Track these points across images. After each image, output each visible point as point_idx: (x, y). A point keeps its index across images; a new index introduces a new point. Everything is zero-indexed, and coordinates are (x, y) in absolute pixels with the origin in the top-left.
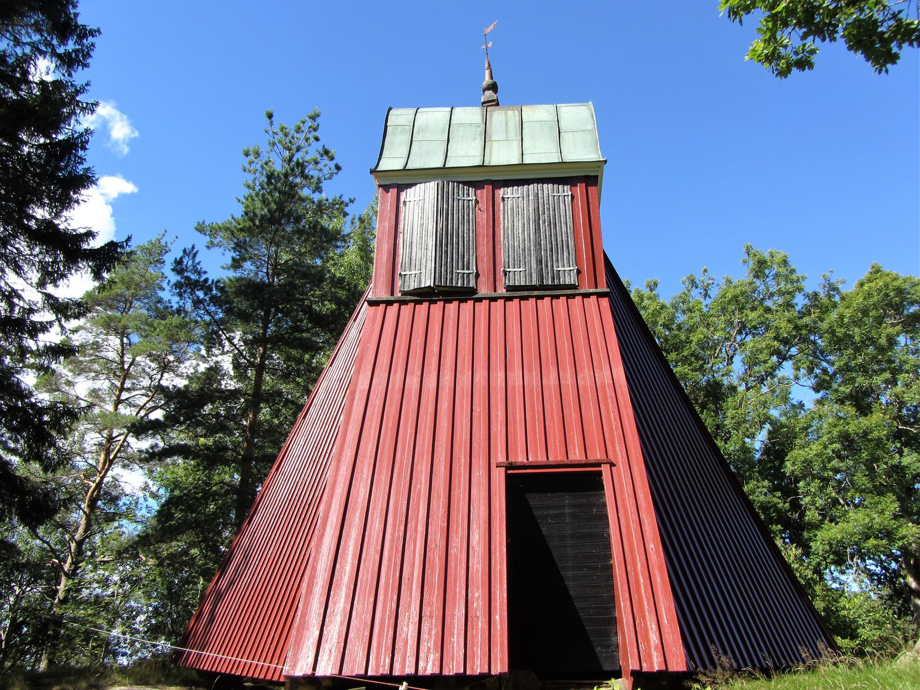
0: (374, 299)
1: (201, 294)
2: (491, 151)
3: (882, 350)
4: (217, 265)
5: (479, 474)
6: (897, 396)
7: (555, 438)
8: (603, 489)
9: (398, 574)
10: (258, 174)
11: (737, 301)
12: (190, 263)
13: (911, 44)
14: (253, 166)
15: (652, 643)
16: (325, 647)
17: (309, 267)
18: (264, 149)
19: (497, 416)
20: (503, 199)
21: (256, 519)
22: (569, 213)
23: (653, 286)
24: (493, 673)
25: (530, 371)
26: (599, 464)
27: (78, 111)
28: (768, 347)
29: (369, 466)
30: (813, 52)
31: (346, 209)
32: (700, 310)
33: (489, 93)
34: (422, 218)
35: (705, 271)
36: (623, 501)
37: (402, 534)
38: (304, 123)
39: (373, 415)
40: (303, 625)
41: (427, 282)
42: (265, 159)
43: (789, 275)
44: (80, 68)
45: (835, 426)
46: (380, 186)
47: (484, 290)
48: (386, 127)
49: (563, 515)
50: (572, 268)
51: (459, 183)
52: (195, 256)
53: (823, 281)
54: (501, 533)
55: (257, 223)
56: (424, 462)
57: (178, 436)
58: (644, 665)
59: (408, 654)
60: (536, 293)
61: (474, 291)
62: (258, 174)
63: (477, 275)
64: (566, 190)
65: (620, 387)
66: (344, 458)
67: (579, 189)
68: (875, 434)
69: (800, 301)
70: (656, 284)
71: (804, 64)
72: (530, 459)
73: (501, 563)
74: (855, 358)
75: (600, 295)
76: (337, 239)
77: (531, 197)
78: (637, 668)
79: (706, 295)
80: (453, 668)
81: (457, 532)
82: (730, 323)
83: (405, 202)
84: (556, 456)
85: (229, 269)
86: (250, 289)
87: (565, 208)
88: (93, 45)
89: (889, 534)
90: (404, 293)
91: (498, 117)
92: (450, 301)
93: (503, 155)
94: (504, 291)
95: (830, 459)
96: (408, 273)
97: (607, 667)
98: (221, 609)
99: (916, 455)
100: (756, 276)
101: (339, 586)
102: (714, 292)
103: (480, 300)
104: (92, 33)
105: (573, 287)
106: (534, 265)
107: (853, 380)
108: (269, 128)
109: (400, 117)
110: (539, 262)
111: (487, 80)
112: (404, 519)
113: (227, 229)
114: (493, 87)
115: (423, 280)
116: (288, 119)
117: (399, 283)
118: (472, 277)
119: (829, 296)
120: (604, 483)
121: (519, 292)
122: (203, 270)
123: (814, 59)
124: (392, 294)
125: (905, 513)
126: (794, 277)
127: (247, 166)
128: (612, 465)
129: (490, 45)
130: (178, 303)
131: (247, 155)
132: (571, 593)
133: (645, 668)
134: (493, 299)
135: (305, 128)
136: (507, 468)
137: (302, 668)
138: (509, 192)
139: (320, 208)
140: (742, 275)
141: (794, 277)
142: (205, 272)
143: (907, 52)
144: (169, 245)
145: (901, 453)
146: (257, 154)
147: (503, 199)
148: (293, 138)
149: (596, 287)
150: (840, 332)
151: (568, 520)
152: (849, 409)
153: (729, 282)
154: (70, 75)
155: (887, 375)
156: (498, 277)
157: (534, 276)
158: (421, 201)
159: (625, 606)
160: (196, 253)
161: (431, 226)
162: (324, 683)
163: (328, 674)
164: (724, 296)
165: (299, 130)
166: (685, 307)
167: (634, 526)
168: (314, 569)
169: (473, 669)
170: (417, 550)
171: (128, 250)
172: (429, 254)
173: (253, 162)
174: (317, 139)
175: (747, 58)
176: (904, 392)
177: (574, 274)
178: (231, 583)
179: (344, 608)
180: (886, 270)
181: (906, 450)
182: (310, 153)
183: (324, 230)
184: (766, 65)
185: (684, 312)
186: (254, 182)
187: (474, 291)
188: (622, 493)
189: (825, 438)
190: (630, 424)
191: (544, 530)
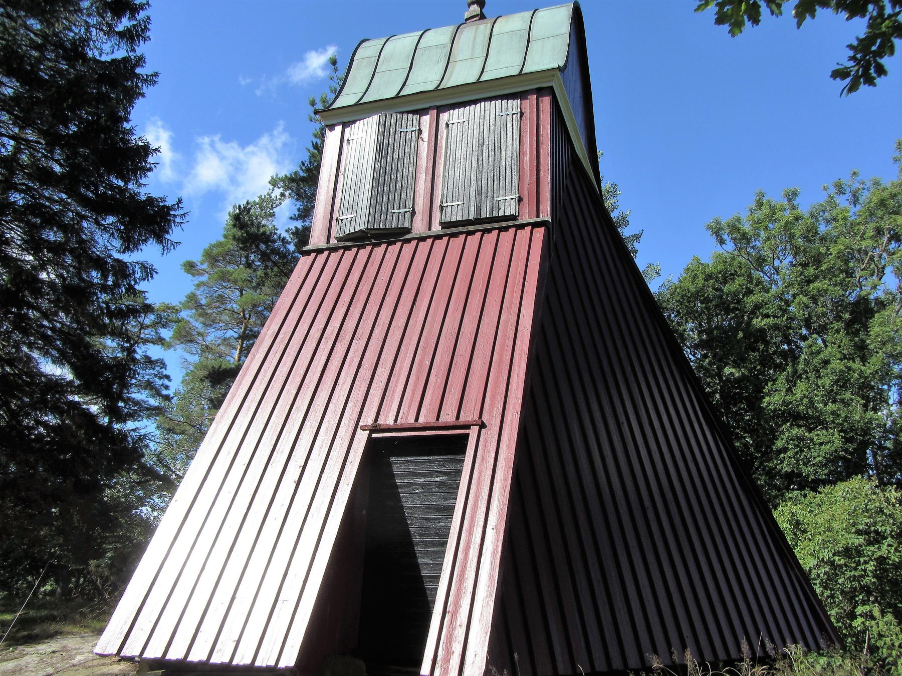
11: (885, 206)
23: (792, 196)
26: (467, 427)
27: (140, 85)
32: (845, 218)
41: (361, 226)
47: (419, 227)
61: (408, 231)
63: (413, 213)
64: (513, 105)
70: (795, 194)
79: (855, 201)
82: (879, 232)
88: (149, 18)
96: (345, 217)
102: (864, 197)
104: (142, 7)
105: (513, 218)
108: (334, 75)
110: (479, 193)
118: (408, 216)
128: (483, 426)
147: (447, 125)
149: (538, 216)
153: (877, 183)
154: (134, 50)
157: (472, 208)
166: (827, 215)
177: (514, 203)
185: (828, 222)
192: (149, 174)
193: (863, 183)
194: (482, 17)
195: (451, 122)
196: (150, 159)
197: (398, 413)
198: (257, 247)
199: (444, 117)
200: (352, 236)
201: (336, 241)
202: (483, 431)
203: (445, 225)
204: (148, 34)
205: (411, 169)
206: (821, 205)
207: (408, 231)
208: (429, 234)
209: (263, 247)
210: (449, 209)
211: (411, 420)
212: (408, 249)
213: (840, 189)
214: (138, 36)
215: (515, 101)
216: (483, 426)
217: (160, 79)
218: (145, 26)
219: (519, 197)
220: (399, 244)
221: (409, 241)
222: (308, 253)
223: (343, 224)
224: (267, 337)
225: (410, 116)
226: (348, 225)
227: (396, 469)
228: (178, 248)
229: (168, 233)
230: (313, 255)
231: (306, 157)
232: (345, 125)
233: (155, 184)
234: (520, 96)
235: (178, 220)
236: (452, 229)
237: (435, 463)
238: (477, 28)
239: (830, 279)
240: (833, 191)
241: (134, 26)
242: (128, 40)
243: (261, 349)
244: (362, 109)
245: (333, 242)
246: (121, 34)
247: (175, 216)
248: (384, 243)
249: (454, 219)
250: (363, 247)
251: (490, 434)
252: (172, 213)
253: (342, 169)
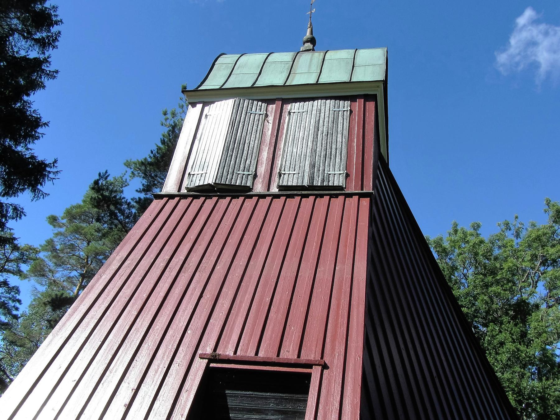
11: (540, 240)
23: (476, 227)
26: (310, 366)
32: (512, 246)
35: (517, 217)
41: (210, 180)
44: (51, 49)
47: (259, 188)
48: (214, 64)
50: (342, 172)
61: (250, 189)
63: (255, 176)
64: (345, 105)
67: (358, 104)
70: (479, 226)
75: (362, 195)
79: (518, 236)
82: (534, 257)
88: (59, 33)
102: (523, 234)
104: (56, 23)
105: (340, 188)
110: (313, 166)
114: (312, 41)
127: (164, 122)
128: (325, 367)
136: (210, 361)
138: (295, 107)
140: (544, 221)
144: (128, 181)
149: (362, 189)
153: (533, 225)
154: (44, 53)
160: (108, 176)
164: (529, 237)
166: (500, 243)
171: (54, 170)
185: (500, 247)
188: (327, 403)
190: (358, 322)
192: (36, 141)
193: (522, 224)
194: (313, 50)
195: (293, 111)
196: (40, 130)
197: (238, 346)
198: (108, 207)
199: (288, 107)
200: (200, 188)
201: (186, 191)
202: (325, 371)
203: (281, 188)
204: (57, 43)
205: (256, 142)
206: (497, 235)
207: (250, 189)
208: (268, 193)
209: (112, 207)
210: (286, 176)
211: (253, 354)
212: (250, 203)
213: (508, 227)
214: (50, 44)
215: (346, 102)
216: (325, 367)
217: (59, 75)
218: (56, 38)
219: (347, 173)
220: (241, 199)
221: (251, 197)
222: (160, 197)
223: (194, 179)
224: (115, 262)
225: (260, 103)
226: (198, 179)
227: (231, 402)
228: (46, 198)
229: (41, 184)
230: (165, 199)
231: (165, 130)
232: (205, 104)
233: (39, 149)
234: (352, 98)
235: (51, 175)
236: (288, 191)
237: (271, 400)
238: (313, 55)
239: (502, 286)
240: (504, 228)
241: (48, 37)
242: (41, 45)
243: (108, 272)
244: (222, 93)
245: (184, 191)
246: (37, 41)
247: (49, 172)
249: (290, 184)
250: (210, 197)
251: (333, 375)
252: (48, 169)
253: (198, 136)
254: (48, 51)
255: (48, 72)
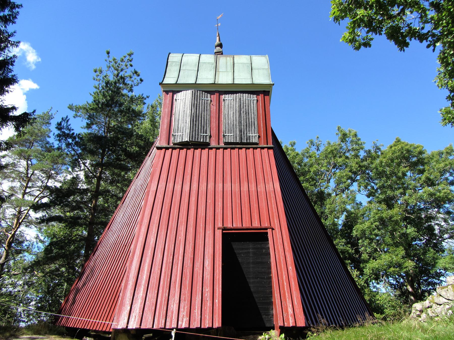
0: (160, 146)
1: (70, 141)
2: (218, 76)
3: (399, 178)
4: (79, 126)
5: (209, 232)
6: (405, 200)
7: (246, 216)
8: (268, 241)
9: (169, 280)
10: (101, 82)
11: (333, 153)
12: (65, 125)
13: (415, 39)
14: (99, 77)
15: (289, 313)
16: (133, 315)
17: (126, 129)
18: (105, 69)
19: (218, 205)
20: (224, 100)
21: (97, 253)
22: (255, 108)
23: (293, 144)
24: (214, 327)
25: (235, 183)
26: (266, 229)
27: (9, 46)
28: (346, 175)
29: (156, 228)
30: (371, 39)
31: (145, 101)
32: (315, 157)
33: (218, 48)
34: (184, 108)
36: (278, 246)
37: (171, 261)
38: (125, 57)
39: (158, 203)
40: (122, 304)
41: (186, 139)
42: (105, 74)
43: (357, 142)
45: (377, 214)
46: (164, 91)
49: (249, 252)
51: (203, 91)
52: (68, 121)
53: (373, 145)
54: (219, 261)
55: (100, 106)
56: (183, 226)
57: (56, 212)
58: (286, 323)
59: (173, 318)
60: (239, 146)
61: (208, 144)
62: (101, 82)
63: (210, 137)
64: (254, 97)
65: (278, 193)
66: (143, 223)
67: (261, 97)
68: (395, 218)
69: (362, 154)
70: (294, 143)
71: (367, 44)
72: (234, 226)
73: (219, 275)
74: (387, 182)
75: (269, 148)
76: (140, 116)
77: (237, 100)
78: (282, 325)
79: (318, 150)
80: (195, 325)
81: (198, 260)
82: (329, 163)
83: (176, 99)
84: (246, 224)
85: (85, 128)
86: (95, 139)
87: (254, 106)
88: (18, 12)
89: (399, 266)
90: (175, 144)
91: (222, 60)
92: (197, 149)
93: (225, 79)
94: (223, 144)
95: (374, 230)
96: (177, 134)
97: (268, 325)
98: (79, 297)
99: (413, 228)
100: (343, 142)
101: (140, 285)
102: (322, 148)
103: (211, 148)
104: (18, 6)
105: (256, 144)
106: (238, 133)
107: (386, 192)
108: (107, 59)
109: (175, 58)
110: (241, 131)
111: (217, 42)
112: (172, 253)
113: (85, 108)
114: (220, 45)
115: (184, 138)
116: (117, 55)
117: (172, 139)
119: (376, 152)
120: (269, 238)
121: (230, 146)
122: (72, 128)
123: (371, 43)
124: (169, 144)
125: (408, 256)
126: (360, 142)
127: (96, 77)
128: (273, 229)
129: (219, 25)
130: (58, 144)
131: (96, 72)
132: (252, 290)
133: (286, 325)
134: (218, 148)
135: (126, 60)
136: (223, 230)
137: (121, 325)
139: (132, 100)
140: (335, 140)
141: (360, 142)
142: (73, 130)
143: (414, 43)
144: (53, 115)
145: (406, 227)
146: (101, 72)
148: (119, 64)
149: (267, 144)
150: (380, 169)
151: (251, 255)
152: (385, 207)
153: (329, 143)
154: (6, 27)
155: (401, 190)
156: (220, 138)
157: (238, 138)
158: (184, 100)
159: (277, 296)
160: (69, 120)
161: (189, 112)
162: (132, 332)
163: (134, 328)
164: (326, 150)
165: (122, 60)
166: (307, 155)
167: (282, 258)
168: (128, 277)
169: (205, 326)
170: (179, 269)
172: (187, 125)
173: (98, 76)
174: (131, 66)
175: (341, 40)
176: (409, 199)
178: (84, 284)
179: (143, 296)
180: (402, 141)
181: (409, 226)
182: (128, 72)
183: (133, 111)
184: (350, 44)
185: (307, 157)
186: (99, 85)
187: (208, 144)
189: (372, 220)
191: (240, 260)
204: (16, 20)
206: (306, 150)
213: (312, 143)
239: (309, 183)
248: (185, 148)
254: (8, 25)
255: (13, 43)
